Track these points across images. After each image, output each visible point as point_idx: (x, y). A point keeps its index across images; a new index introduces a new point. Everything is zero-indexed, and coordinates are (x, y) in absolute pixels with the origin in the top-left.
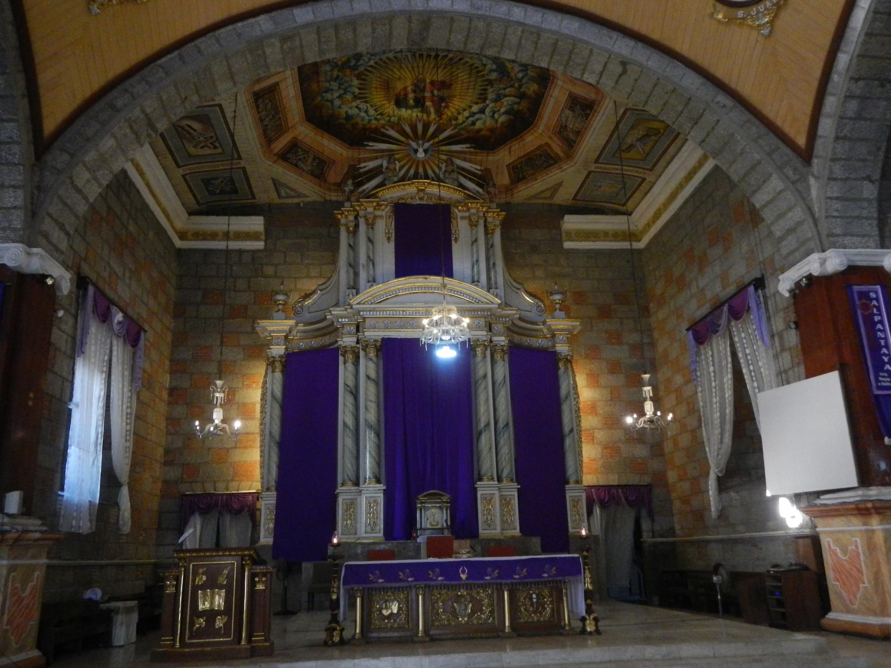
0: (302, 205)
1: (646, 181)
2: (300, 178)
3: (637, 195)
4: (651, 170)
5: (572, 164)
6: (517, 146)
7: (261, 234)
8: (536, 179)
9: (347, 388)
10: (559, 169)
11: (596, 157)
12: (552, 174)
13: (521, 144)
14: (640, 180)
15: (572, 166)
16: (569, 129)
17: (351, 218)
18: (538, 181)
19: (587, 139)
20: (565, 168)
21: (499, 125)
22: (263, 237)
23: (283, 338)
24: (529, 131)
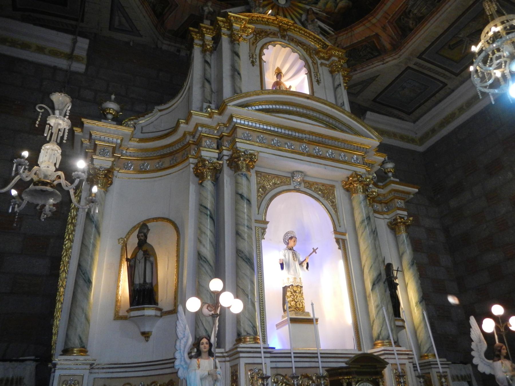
0: (131, 44)
1: (446, 87)
2: (141, 7)
3: (428, 104)
4: (457, 75)
5: (396, 56)
6: (345, 36)
7: (83, 59)
8: (356, 70)
9: (204, 210)
10: (381, 61)
11: (423, 49)
12: (373, 66)
13: (350, 34)
14: (441, 85)
15: (395, 59)
16: (411, 15)
17: (208, 37)
18: (356, 72)
19: (429, 24)
20: (387, 60)
21: (336, 11)
22: (85, 61)
23: (111, 149)
24: (361, 22)
